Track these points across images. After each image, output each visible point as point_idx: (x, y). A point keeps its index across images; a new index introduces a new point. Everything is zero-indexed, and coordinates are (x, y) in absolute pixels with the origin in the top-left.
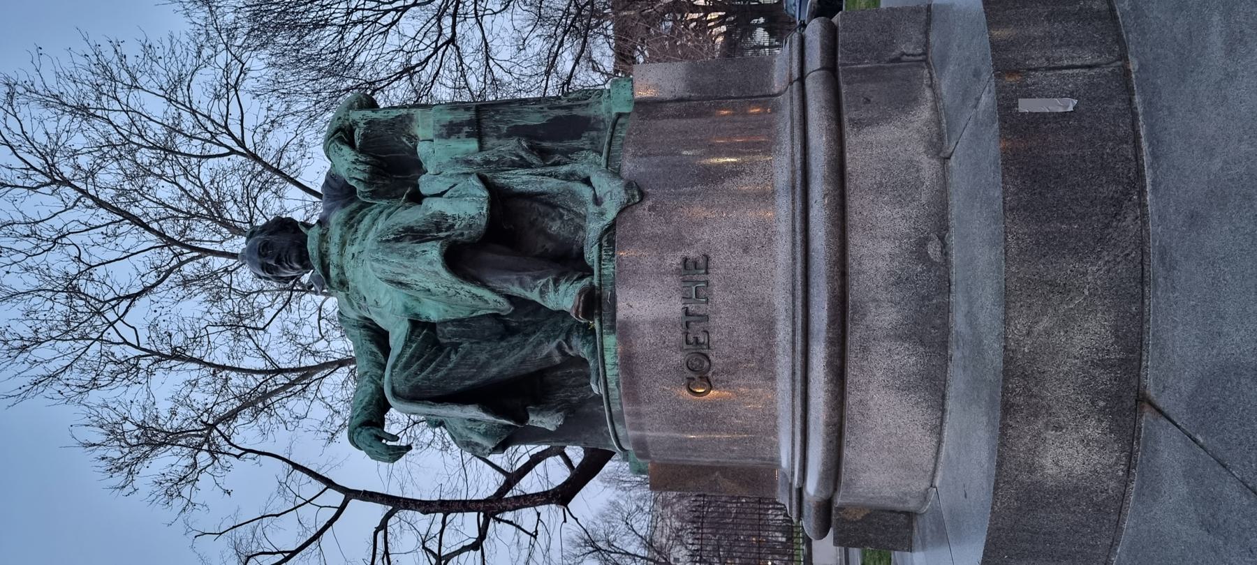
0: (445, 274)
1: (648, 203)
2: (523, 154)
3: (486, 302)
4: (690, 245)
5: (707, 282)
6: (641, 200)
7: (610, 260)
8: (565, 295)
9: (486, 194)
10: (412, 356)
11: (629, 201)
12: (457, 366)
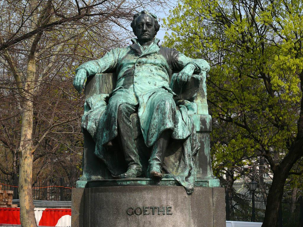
0: (162, 128)
1: (187, 196)
2: (196, 148)
3: (151, 138)
4: (175, 209)
5: (164, 214)
6: (188, 194)
7: (169, 184)
8: (157, 168)
9: (185, 137)
10: (129, 108)
11: (188, 190)
12: (127, 125)
